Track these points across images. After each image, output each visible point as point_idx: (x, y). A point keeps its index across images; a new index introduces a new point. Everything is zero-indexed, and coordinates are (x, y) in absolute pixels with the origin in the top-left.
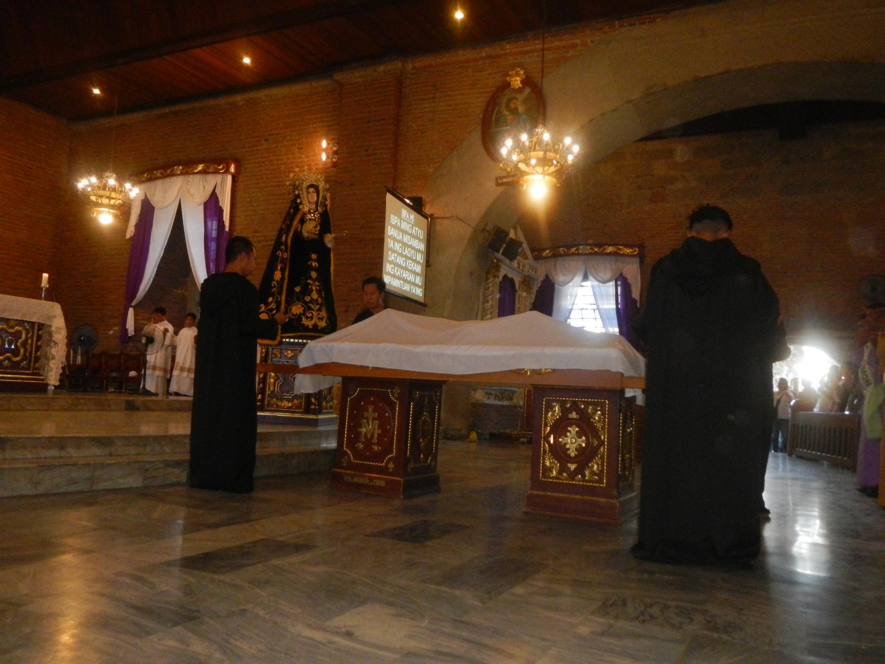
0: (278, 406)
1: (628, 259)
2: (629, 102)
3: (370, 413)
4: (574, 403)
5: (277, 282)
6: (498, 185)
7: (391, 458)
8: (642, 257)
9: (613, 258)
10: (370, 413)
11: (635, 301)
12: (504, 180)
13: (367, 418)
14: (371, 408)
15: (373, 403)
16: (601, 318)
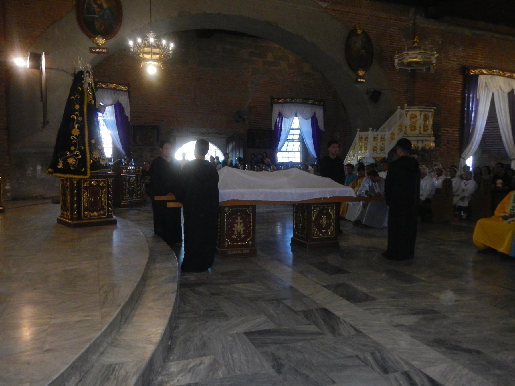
0: (90, 216)
1: (122, 93)
2: (171, 17)
3: (239, 220)
4: (324, 207)
5: (76, 136)
6: (92, 52)
7: (250, 240)
8: (129, 92)
9: (112, 91)
10: (239, 220)
11: (127, 117)
12: (97, 50)
13: (237, 223)
14: (239, 218)
15: (239, 216)
16: (106, 125)
